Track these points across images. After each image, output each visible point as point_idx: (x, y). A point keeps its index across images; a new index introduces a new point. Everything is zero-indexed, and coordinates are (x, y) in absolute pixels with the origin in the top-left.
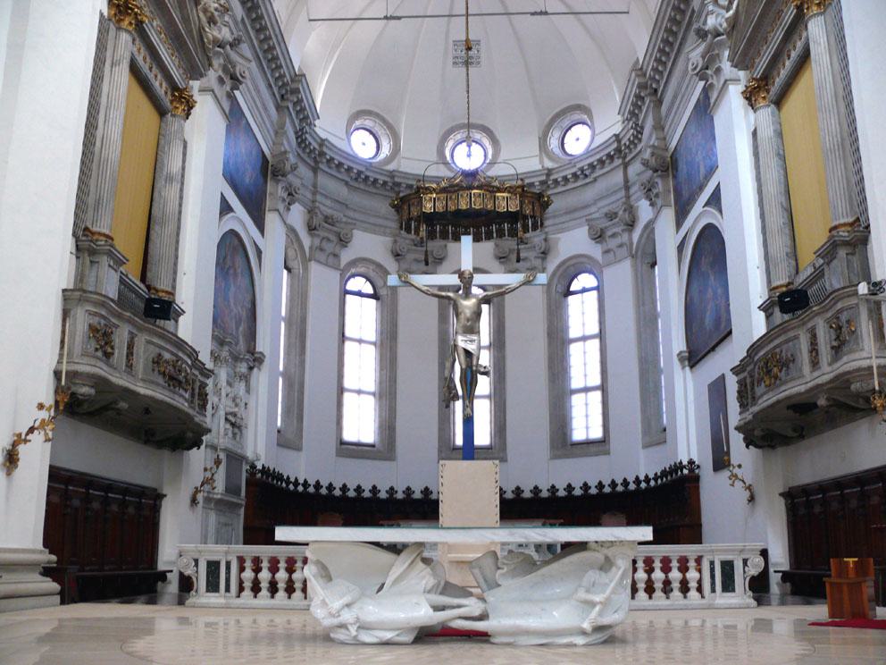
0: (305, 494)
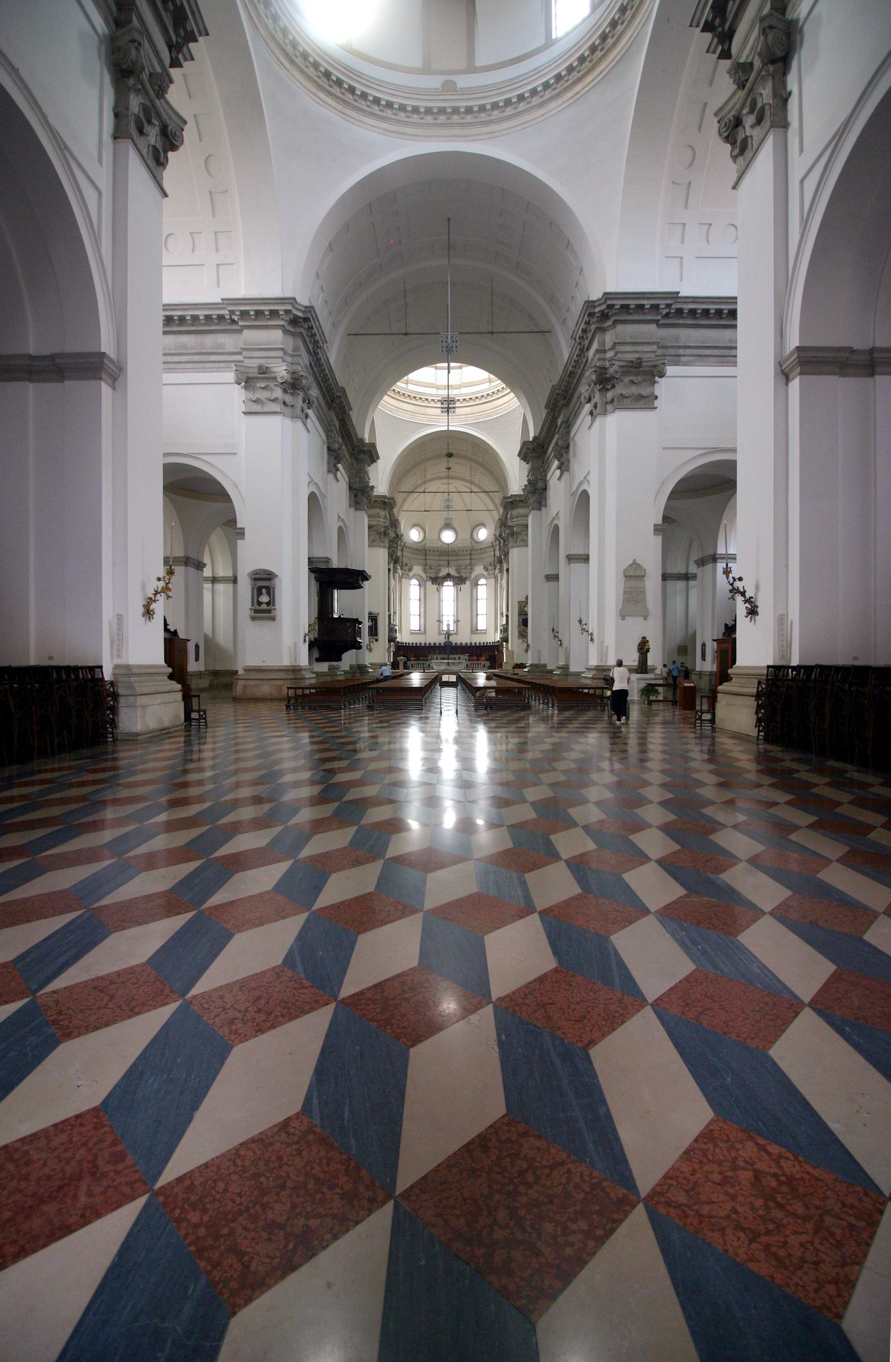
0: (406, 646)
